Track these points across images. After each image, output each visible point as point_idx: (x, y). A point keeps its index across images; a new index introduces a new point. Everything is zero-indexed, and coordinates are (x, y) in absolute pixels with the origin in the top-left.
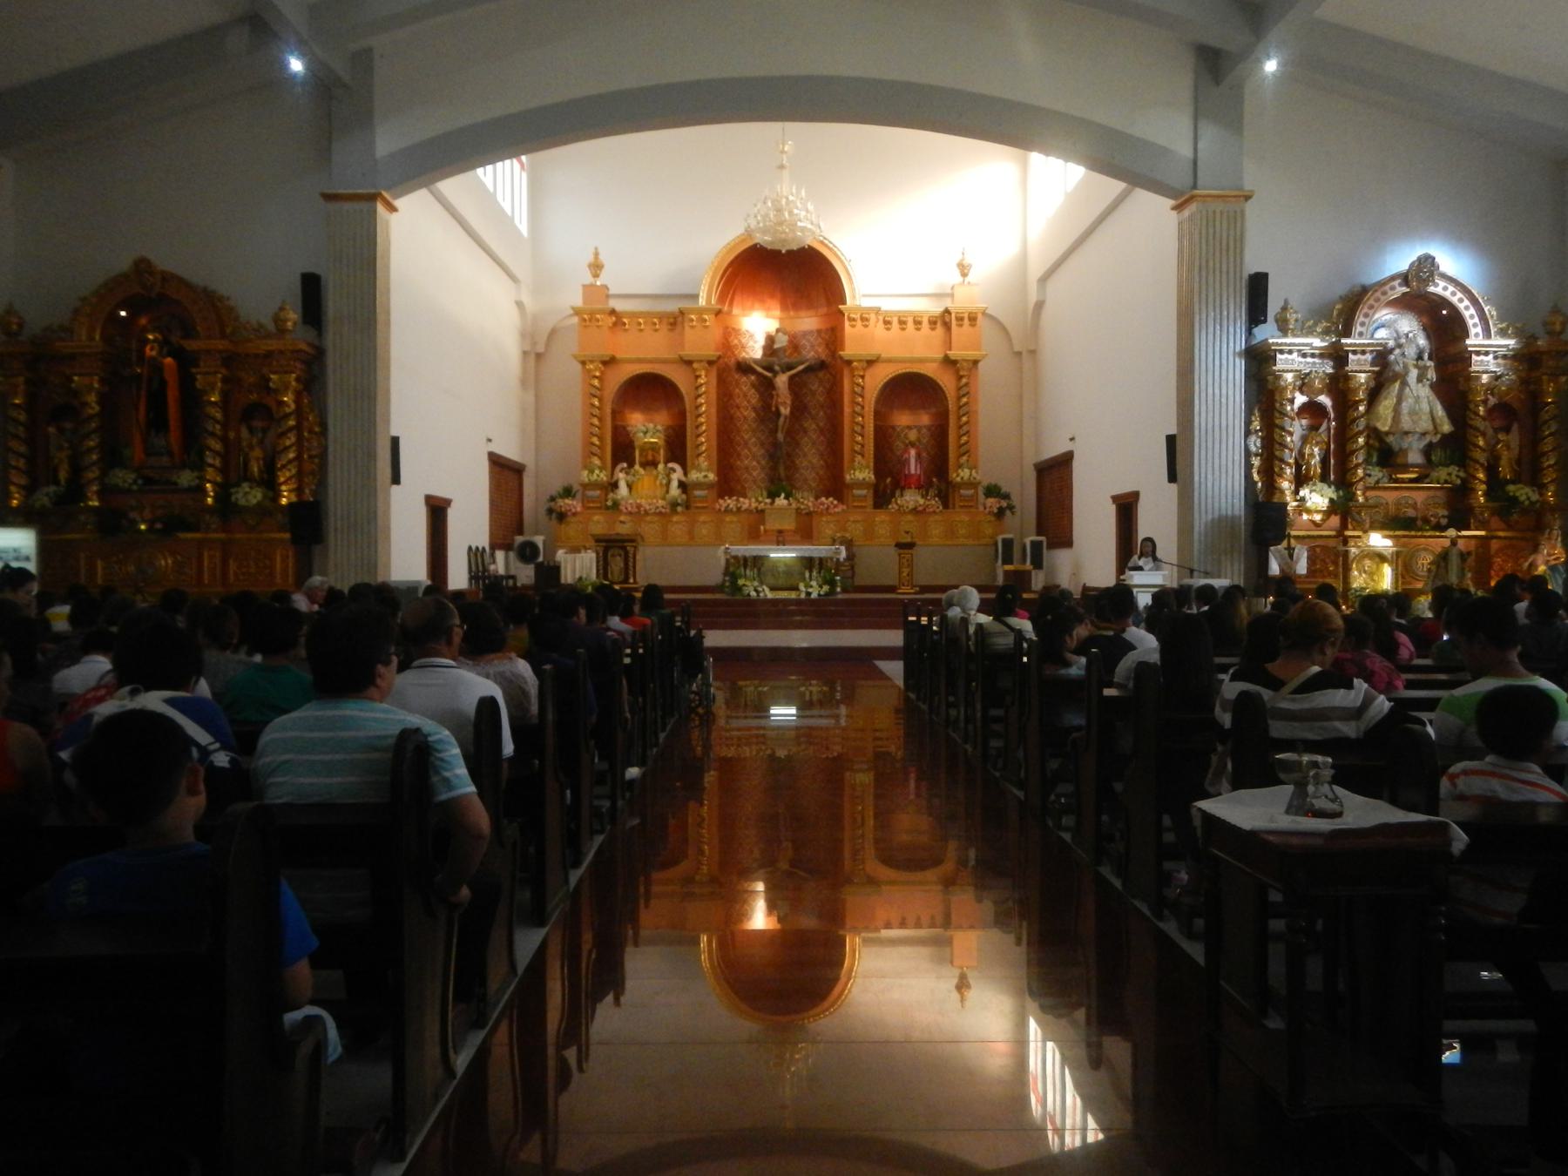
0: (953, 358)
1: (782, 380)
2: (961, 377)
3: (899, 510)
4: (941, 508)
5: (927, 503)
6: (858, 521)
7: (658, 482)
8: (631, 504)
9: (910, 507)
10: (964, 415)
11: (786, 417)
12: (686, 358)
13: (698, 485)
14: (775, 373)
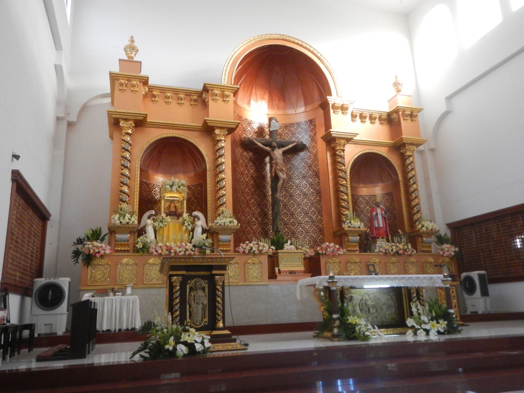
0: (405, 141)
1: (278, 153)
2: (409, 156)
3: (386, 253)
4: (415, 251)
5: (406, 247)
6: (355, 263)
7: (184, 228)
8: (160, 247)
9: (394, 251)
10: (414, 183)
11: (284, 180)
12: (210, 124)
13: (225, 230)
14: (273, 148)
